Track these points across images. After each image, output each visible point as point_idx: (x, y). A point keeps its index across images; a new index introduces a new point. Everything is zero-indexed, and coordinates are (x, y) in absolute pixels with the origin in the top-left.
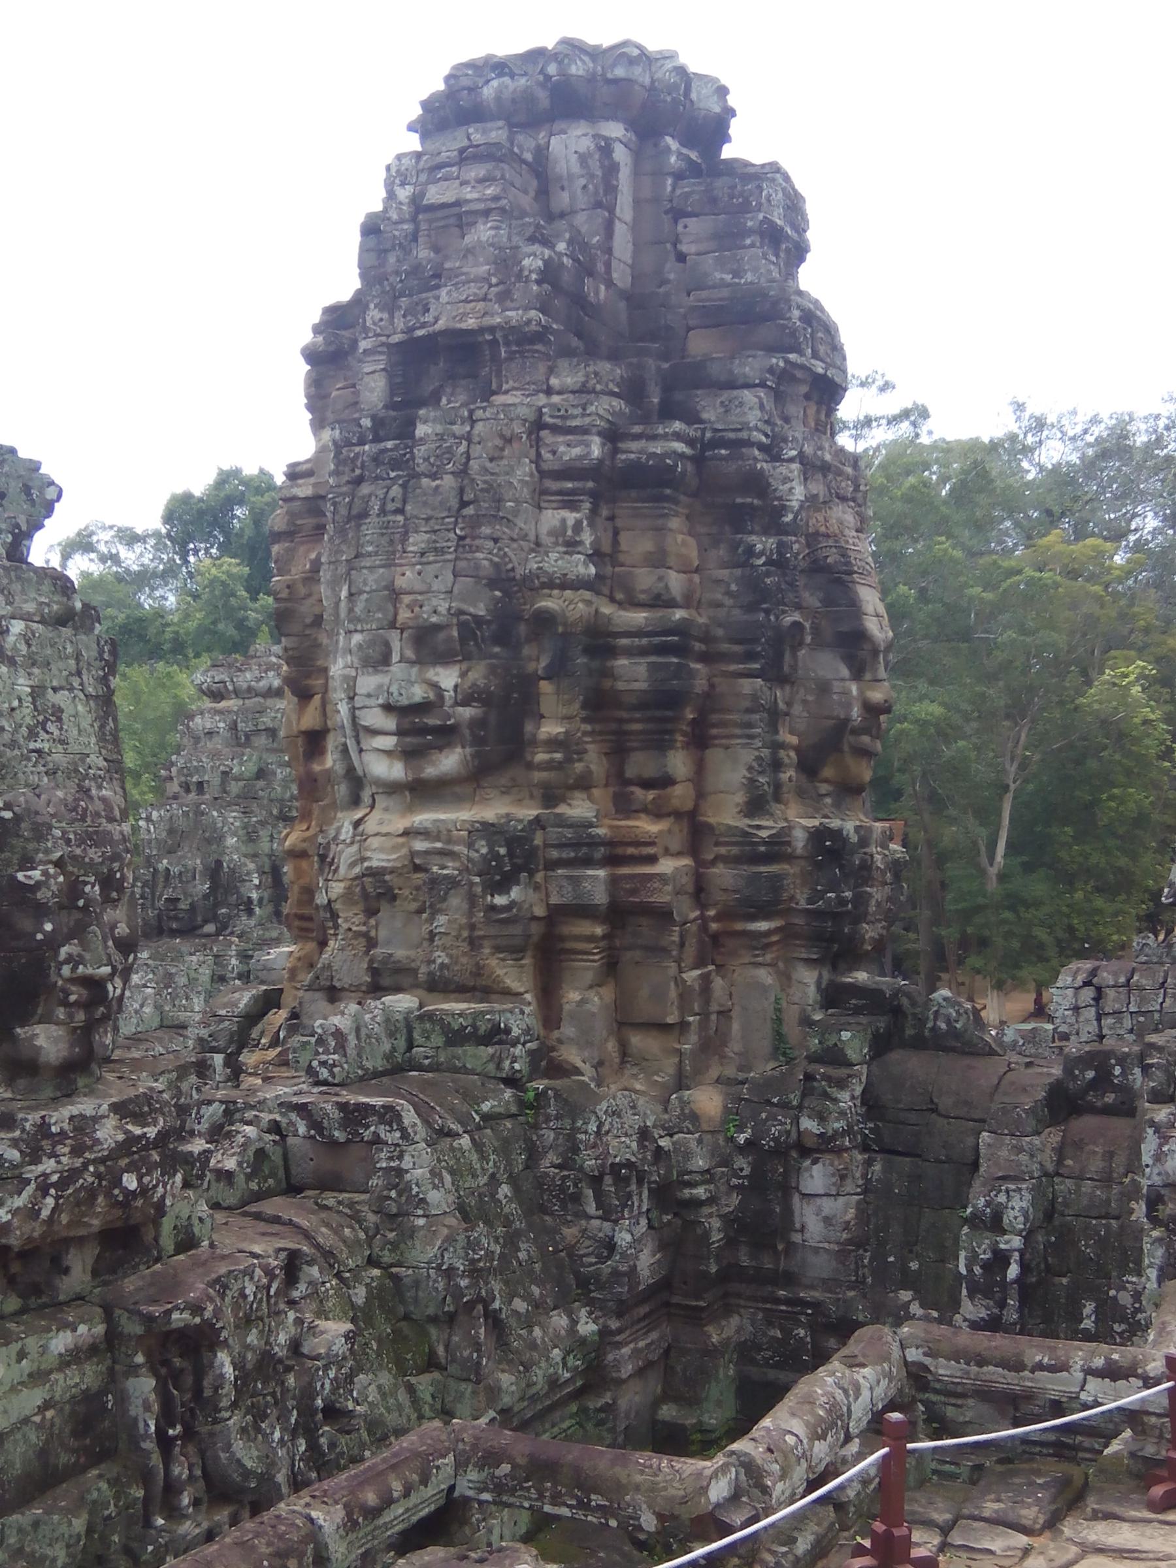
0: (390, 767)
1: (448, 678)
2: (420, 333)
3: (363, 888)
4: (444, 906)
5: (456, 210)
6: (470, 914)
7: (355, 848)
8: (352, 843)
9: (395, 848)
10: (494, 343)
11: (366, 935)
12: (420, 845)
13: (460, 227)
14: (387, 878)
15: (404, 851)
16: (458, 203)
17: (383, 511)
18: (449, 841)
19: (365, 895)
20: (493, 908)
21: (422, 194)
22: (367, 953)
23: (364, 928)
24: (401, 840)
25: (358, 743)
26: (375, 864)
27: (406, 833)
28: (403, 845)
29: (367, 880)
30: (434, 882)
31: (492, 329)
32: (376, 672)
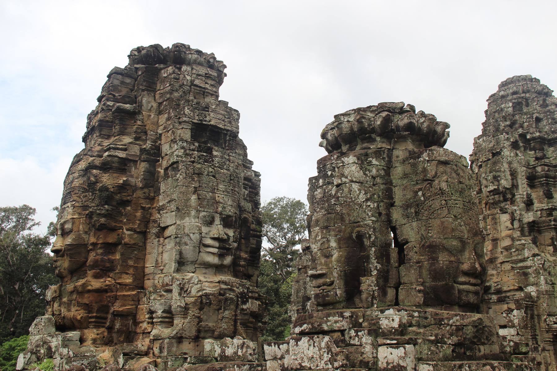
0: (214, 259)
1: (231, 233)
2: (204, 123)
3: (202, 300)
4: (228, 308)
5: (203, 90)
6: (235, 311)
7: (199, 286)
8: (197, 284)
9: (215, 287)
10: (227, 134)
11: (199, 317)
12: (223, 286)
13: (203, 95)
14: (210, 297)
15: (218, 288)
16: (204, 88)
17: (208, 175)
18: (232, 286)
19: (201, 302)
20: (243, 309)
21: (194, 81)
22: (198, 324)
23: (199, 315)
24: (217, 284)
25: (199, 249)
26: (208, 292)
27: (219, 282)
28: (218, 286)
29: (203, 297)
30: (226, 300)
31: (228, 130)
32: (208, 226)
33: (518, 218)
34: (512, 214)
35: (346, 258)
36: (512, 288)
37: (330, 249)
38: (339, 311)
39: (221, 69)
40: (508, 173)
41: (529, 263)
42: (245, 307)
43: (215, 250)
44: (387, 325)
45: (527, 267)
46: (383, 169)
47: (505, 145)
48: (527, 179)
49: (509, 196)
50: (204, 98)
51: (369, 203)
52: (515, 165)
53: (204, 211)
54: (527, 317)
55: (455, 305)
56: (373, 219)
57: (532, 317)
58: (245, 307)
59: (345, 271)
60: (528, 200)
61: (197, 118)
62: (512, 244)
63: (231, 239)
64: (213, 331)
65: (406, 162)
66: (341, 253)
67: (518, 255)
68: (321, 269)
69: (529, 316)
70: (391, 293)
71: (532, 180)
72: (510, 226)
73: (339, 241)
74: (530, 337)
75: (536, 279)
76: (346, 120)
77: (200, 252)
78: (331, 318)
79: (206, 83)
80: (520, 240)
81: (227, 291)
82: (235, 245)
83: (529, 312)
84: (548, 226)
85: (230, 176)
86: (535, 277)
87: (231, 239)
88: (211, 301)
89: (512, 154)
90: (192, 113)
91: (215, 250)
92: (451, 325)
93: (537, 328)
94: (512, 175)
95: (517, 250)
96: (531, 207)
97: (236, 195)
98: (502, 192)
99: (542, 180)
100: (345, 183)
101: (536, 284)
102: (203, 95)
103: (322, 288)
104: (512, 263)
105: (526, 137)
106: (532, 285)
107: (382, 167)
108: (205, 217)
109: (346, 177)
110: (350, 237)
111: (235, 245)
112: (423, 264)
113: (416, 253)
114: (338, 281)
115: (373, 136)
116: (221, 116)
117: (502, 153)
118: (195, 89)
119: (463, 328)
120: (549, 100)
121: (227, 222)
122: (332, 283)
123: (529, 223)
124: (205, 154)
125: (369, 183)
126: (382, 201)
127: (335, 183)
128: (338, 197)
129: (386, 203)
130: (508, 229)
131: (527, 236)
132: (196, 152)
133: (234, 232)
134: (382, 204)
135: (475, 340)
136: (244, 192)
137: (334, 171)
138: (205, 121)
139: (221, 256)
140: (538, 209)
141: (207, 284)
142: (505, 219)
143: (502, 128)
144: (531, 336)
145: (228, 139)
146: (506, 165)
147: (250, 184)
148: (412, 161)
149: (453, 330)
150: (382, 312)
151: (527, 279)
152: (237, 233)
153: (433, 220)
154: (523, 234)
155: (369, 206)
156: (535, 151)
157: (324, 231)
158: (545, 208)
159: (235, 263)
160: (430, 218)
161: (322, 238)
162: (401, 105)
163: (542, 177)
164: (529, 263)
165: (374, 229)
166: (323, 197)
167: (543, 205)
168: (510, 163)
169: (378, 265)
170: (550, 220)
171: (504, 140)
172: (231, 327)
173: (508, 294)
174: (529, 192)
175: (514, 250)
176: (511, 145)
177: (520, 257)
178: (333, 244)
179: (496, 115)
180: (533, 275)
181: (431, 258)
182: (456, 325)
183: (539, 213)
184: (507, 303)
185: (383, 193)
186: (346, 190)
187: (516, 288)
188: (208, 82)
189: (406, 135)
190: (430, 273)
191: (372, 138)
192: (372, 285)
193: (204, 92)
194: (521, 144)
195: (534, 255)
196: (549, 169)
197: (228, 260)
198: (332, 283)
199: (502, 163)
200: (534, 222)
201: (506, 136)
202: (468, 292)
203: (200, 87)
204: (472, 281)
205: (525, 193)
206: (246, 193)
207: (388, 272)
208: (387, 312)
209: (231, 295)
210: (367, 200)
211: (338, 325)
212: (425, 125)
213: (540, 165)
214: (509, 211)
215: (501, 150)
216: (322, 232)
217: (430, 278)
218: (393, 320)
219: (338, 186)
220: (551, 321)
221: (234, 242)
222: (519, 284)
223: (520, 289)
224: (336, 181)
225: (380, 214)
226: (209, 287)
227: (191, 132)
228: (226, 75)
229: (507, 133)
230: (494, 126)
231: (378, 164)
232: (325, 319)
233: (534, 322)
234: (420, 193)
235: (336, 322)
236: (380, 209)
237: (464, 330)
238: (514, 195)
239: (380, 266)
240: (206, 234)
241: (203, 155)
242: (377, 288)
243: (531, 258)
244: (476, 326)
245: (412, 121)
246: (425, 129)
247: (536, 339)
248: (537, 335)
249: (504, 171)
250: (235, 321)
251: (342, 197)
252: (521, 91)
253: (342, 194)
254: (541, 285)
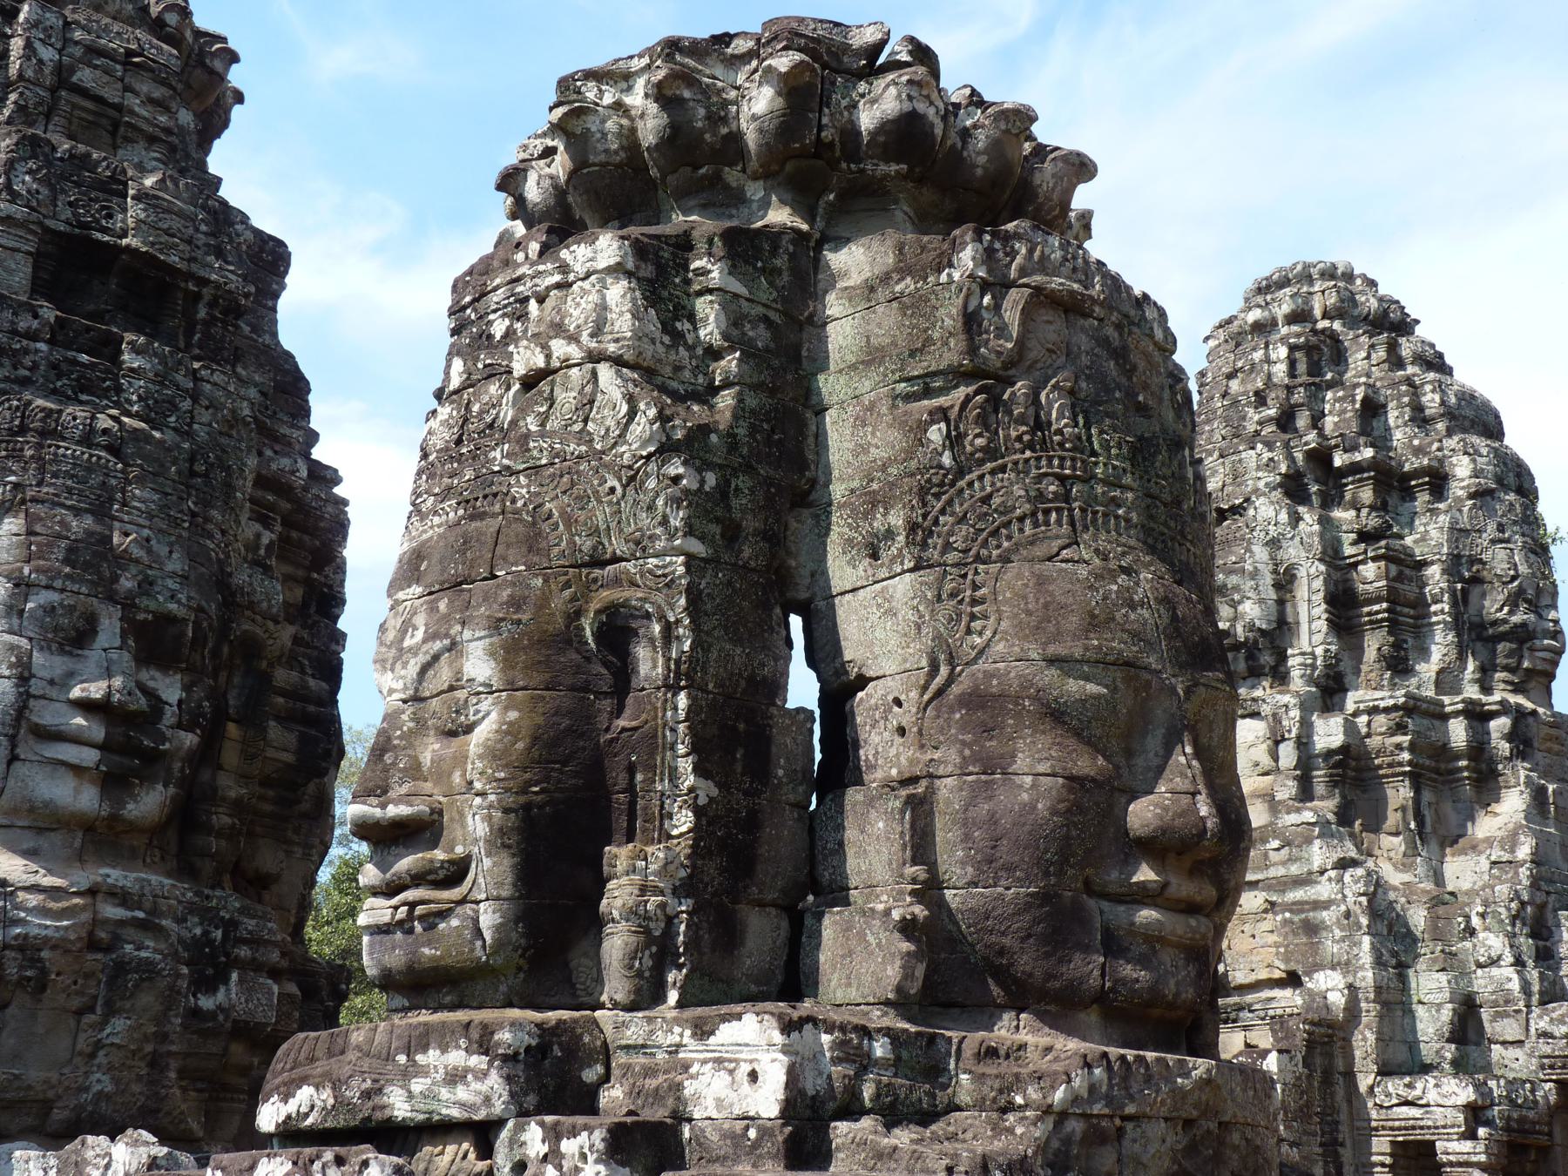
0: (77, 791)
1: (171, 690)
2: (99, 235)
4: (128, 1005)
5: (112, 112)
10: (197, 297)
12: (112, 912)
13: (114, 134)
14: (45, 954)
15: (85, 917)
16: (119, 108)
18: (154, 911)
20: (196, 1013)
21: (72, 71)
25: (14, 746)
27: (92, 892)
28: (84, 908)
30: (120, 969)
31: (204, 282)
32: (62, 652)
33: (1293, 735)
34: (1276, 718)
35: (535, 739)
36: (1263, 974)
37: (461, 694)
38: (478, 1016)
39: (218, 65)
40: (1268, 579)
41: (1324, 889)
42: (206, 1003)
43: (89, 756)
44: (719, 1103)
45: (1318, 905)
46: (766, 319)
47: (1261, 484)
48: (1327, 602)
49: (1267, 659)
50: (115, 147)
52: (1292, 552)
53: (47, 587)
54: (1310, 1077)
55: (1085, 1006)
56: (697, 547)
57: (1327, 1080)
58: (206, 1003)
60: (1327, 676)
61: (68, 213)
62: (1271, 824)
63: (170, 716)
64: (47, 1106)
65: (882, 294)
66: (513, 715)
67: (1291, 860)
68: (407, 798)
69: (1318, 1075)
70: (761, 932)
71: (1343, 605)
72: (1266, 761)
73: (507, 655)
74: (1320, 1150)
75: (1345, 945)
76: (608, 99)
77: (13, 759)
78: (431, 1058)
79: (127, 89)
80: (1298, 810)
81: (130, 933)
82: (189, 739)
83: (1318, 1061)
84: (1390, 765)
85: (192, 459)
86: (1343, 939)
87: (170, 716)
88: (44, 972)
89: (1284, 517)
90: (45, 191)
91: (89, 756)
93: (1343, 1117)
94: (1278, 586)
95: (1287, 843)
96: (1336, 699)
97: (211, 537)
98: (1244, 644)
99: (1376, 608)
100: (567, 364)
101: (1345, 966)
102: (114, 134)
103: (410, 895)
104: (1269, 888)
105: (1331, 460)
106: (1333, 968)
107: (760, 310)
108: (50, 610)
109: (573, 338)
110: (569, 637)
111: (189, 739)
112: (931, 791)
113: (901, 731)
114: (487, 862)
115: (732, 176)
116: (175, 223)
117: (1251, 512)
118: (74, 106)
119: (1120, 1132)
120: (1406, 348)
121: (153, 642)
122: (456, 872)
123: (1329, 753)
124: (84, 358)
125: (687, 374)
126: (748, 468)
127: (519, 369)
128: (527, 436)
129: (768, 482)
130: (1260, 769)
131: (1322, 798)
132: (42, 346)
133: (187, 688)
134: (742, 482)
136: (258, 536)
137: (522, 316)
138: (105, 230)
139: (114, 782)
140: (1362, 706)
141: (33, 900)
142: (1251, 738)
143: (1251, 427)
144: (1321, 1145)
145: (202, 313)
146: (1261, 553)
147: (286, 506)
148: (907, 285)
150: (703, 1031)
151: (1314, 947)
152: (198, 693)
153: (994, 568)
154: (1306, 793)
156: (1358, 510)
157: (443, 606)
158: (1382, 704)
159: (186, 817)
160: (978, 559)
161: (430, 637)
162: (870, 36)
163: (1378, 600)
164: (1324, 889)
166: (459, 442)
167: (1378, 694)
168: (1274, 544)
170: (1399, 747)
171: (1258, 468)
172: (136, 1088)
173: (1249, 998)
174: (1333, 648)
175: (1275, 844)
176: (1280, 485)
177: (1295, 869)
178: (479, 665)
179: (1235, 385)
180: (1338, 933)
181: (975, 759)
182: (1084, 1116)
183: (1364, 719)
184: (1246, 1028)
185: (753, 430)
186: (567, 398)
187: (1277, 974)
188: (137, 86)
189: (886, 176)
190: (967, 837)
191: (727, 187)
193: (116, 125)
194: (1314, 488)
195: (1344, 864)
196: (1400, 573)
197: (148, 803)
198: (456, 872)
199: (1250, 543)
200: (1344, 749)
201: (1267, 455)
203: (99, 100)
205: (1319, 651)
206: (265, 541)
207: (752, 823)
208: (727, 1033)
209: (150, 950)
211: (462, 1093)
212: (981, 140)
213: (1374, 559)
214: (1266, 709)
215: (1247, 500)
216: (433, 609)
217: (963, 863)
218: (753, 1076)
219: (531, 381)
220: (1388, 1095)
221: (179, 726)
222: (1287, 960)
223: (1292, 980)
224: (525, 359)
225: (732, 534)
226: (42, 911)
227: (36, 267)
228: (239, 98)
229: (1269, 445)
230: (1227, 421)
231: (743, 291)
232: (402, 1059)
233: (1332, 1094)
234: (936, 433)
235: (455, 1077)
236: (735, 503)
237: (1126, 1143)
238: (1282, 657)
239: (715, 792)
240: (52, 682)
241: (75, 362)
243: (1333, 874)
244: (1188, 1123)
245: (921, 107)
246: (982, 159)
247: (1337, 1155)
248: (1342, 1145)
249: (1254, 575)
250: (156, 1063)
251: (543, 434)
252: (1318, 313)
253: (544, 419)
254: (1362, 968)
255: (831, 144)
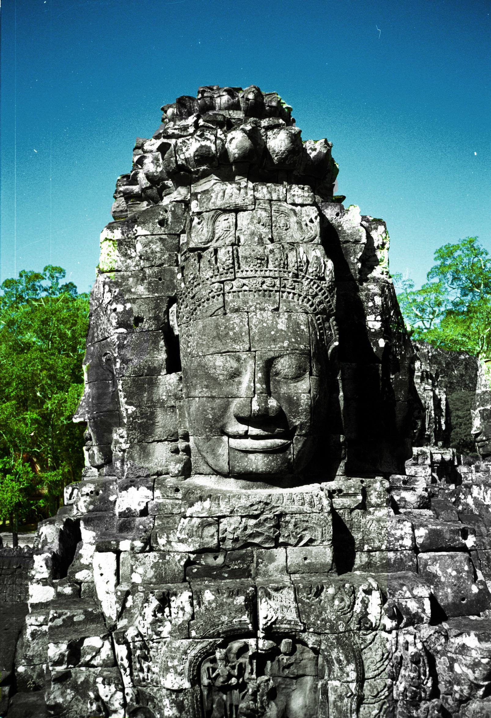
51: (114, 306)
59: (93, 418)
92: (191, 517)
135: (257, 540)
149: (193, 526)
155: (115, 310)
165: (121, 347)
169: (127, 407)
192: (122, 440)
202: (247, 452)
204: (254, 431)
207: (152, 416)
210: (116, 299)
231: (149, 233)
242: (128, 445)
245: (204, 143)
255: (183, 165)
